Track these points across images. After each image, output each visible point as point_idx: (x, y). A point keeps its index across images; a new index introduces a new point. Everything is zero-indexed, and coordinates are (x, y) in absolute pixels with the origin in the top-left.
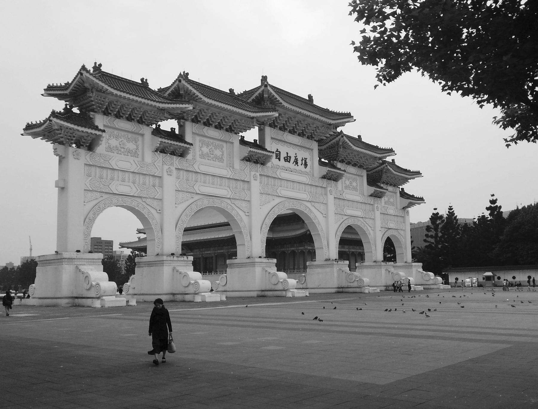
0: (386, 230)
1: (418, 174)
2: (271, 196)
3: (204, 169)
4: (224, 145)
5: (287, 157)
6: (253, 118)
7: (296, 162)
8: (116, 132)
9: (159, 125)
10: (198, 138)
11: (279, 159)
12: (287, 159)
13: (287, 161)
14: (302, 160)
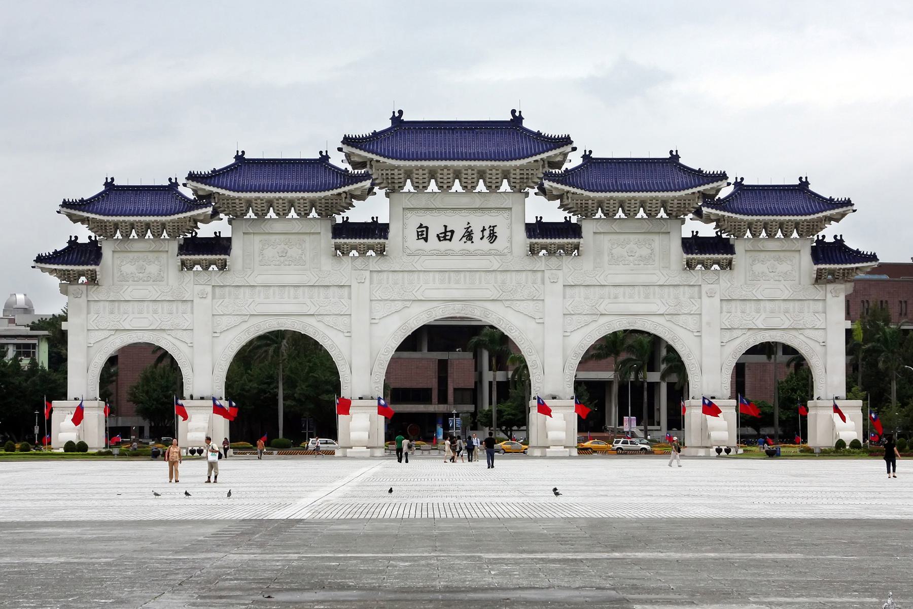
0: (751, 332)
1: (848, 203)
2: (400, 303)
3: (260, 280)
4: (306, 237)
5: (446, 231)
6: (339, 194)
7: (469, 236)
8: (131, 255)
9: (196, 233)
10: (257, 238)
11: (426, 239)
12: (446, 235)
13: (445, 239)
14: (484, 229)
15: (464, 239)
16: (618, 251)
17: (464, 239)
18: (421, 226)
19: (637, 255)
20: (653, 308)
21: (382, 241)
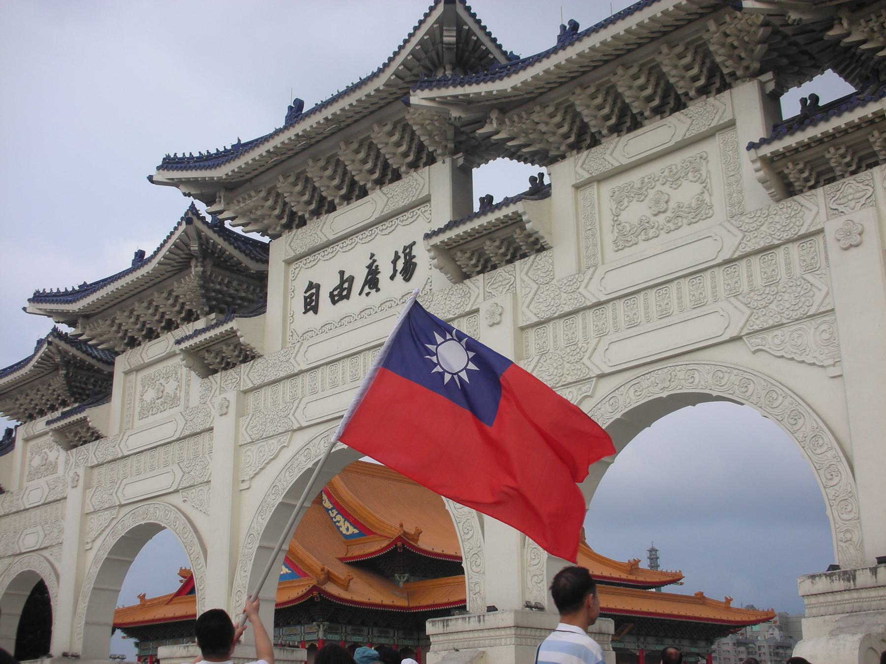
2: (274, 441)
5: (342, 282)
11: (315, 310)
13: (342, 298)
14: (397, 257)
15: (367, 289)
16: (635, 212)
17: (367, 289)
18: (311, 286)
19: (672, 204)
20: (706, 328)
21: (226, 327)
